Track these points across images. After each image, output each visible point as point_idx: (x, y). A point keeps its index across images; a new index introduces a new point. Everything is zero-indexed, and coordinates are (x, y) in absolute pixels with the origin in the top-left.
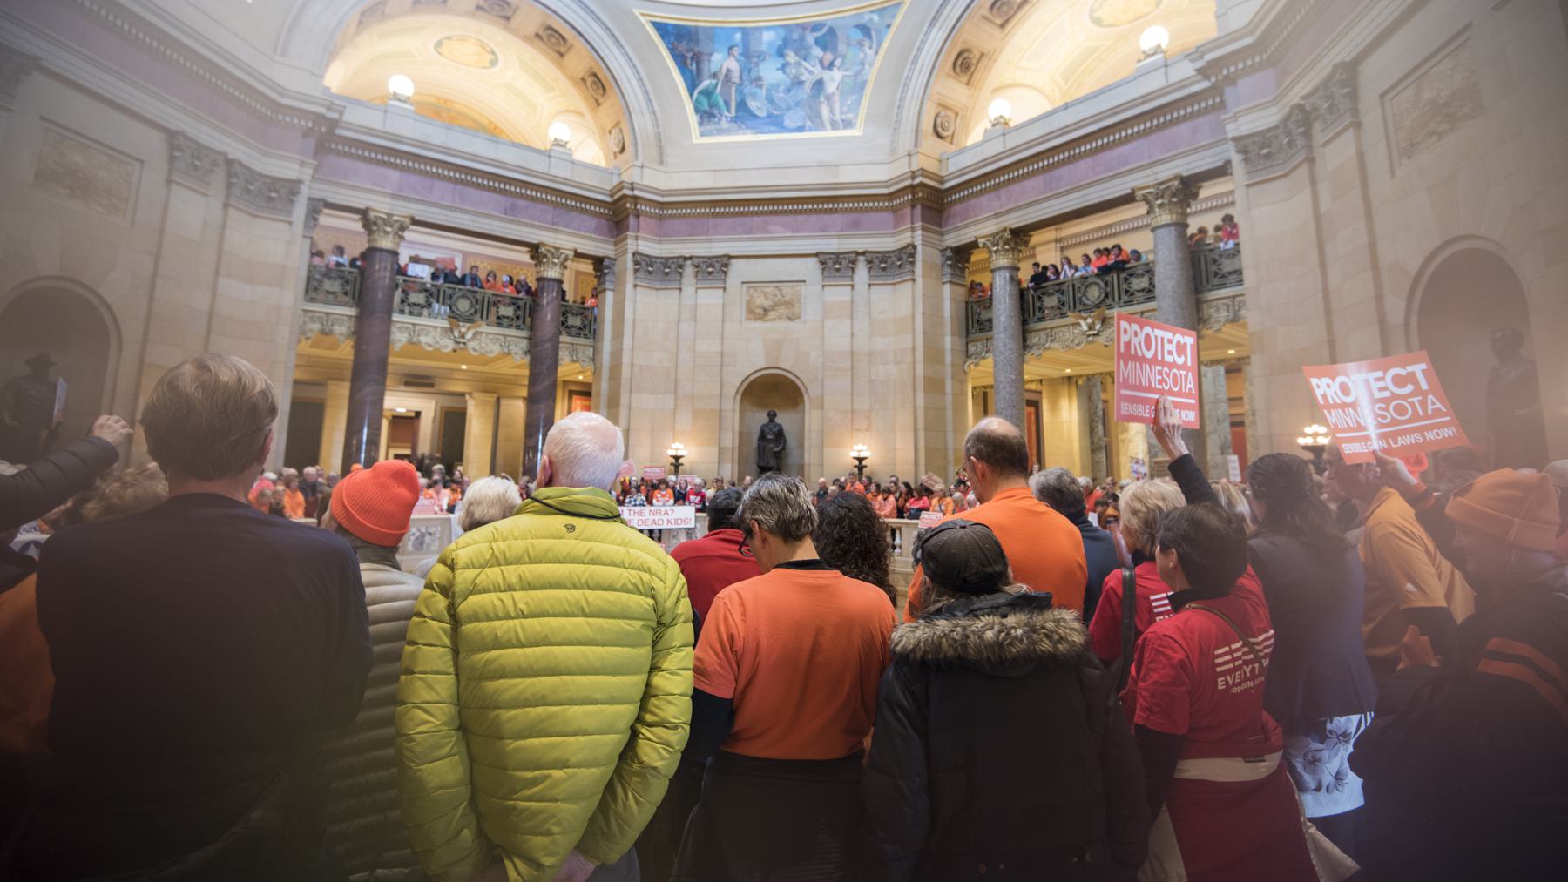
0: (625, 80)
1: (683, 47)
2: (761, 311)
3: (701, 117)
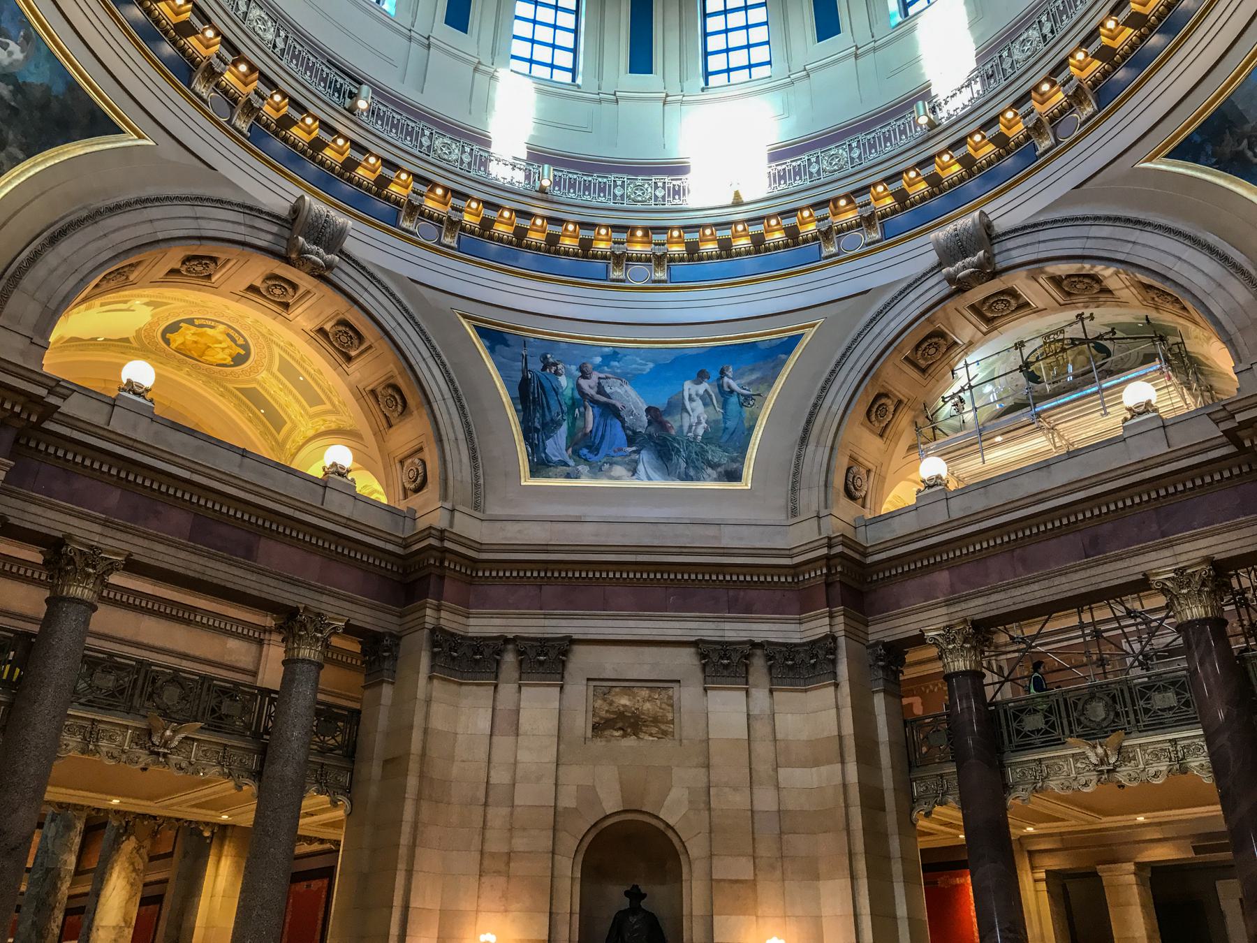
0: (1169, 262)
1: (1228, 147)
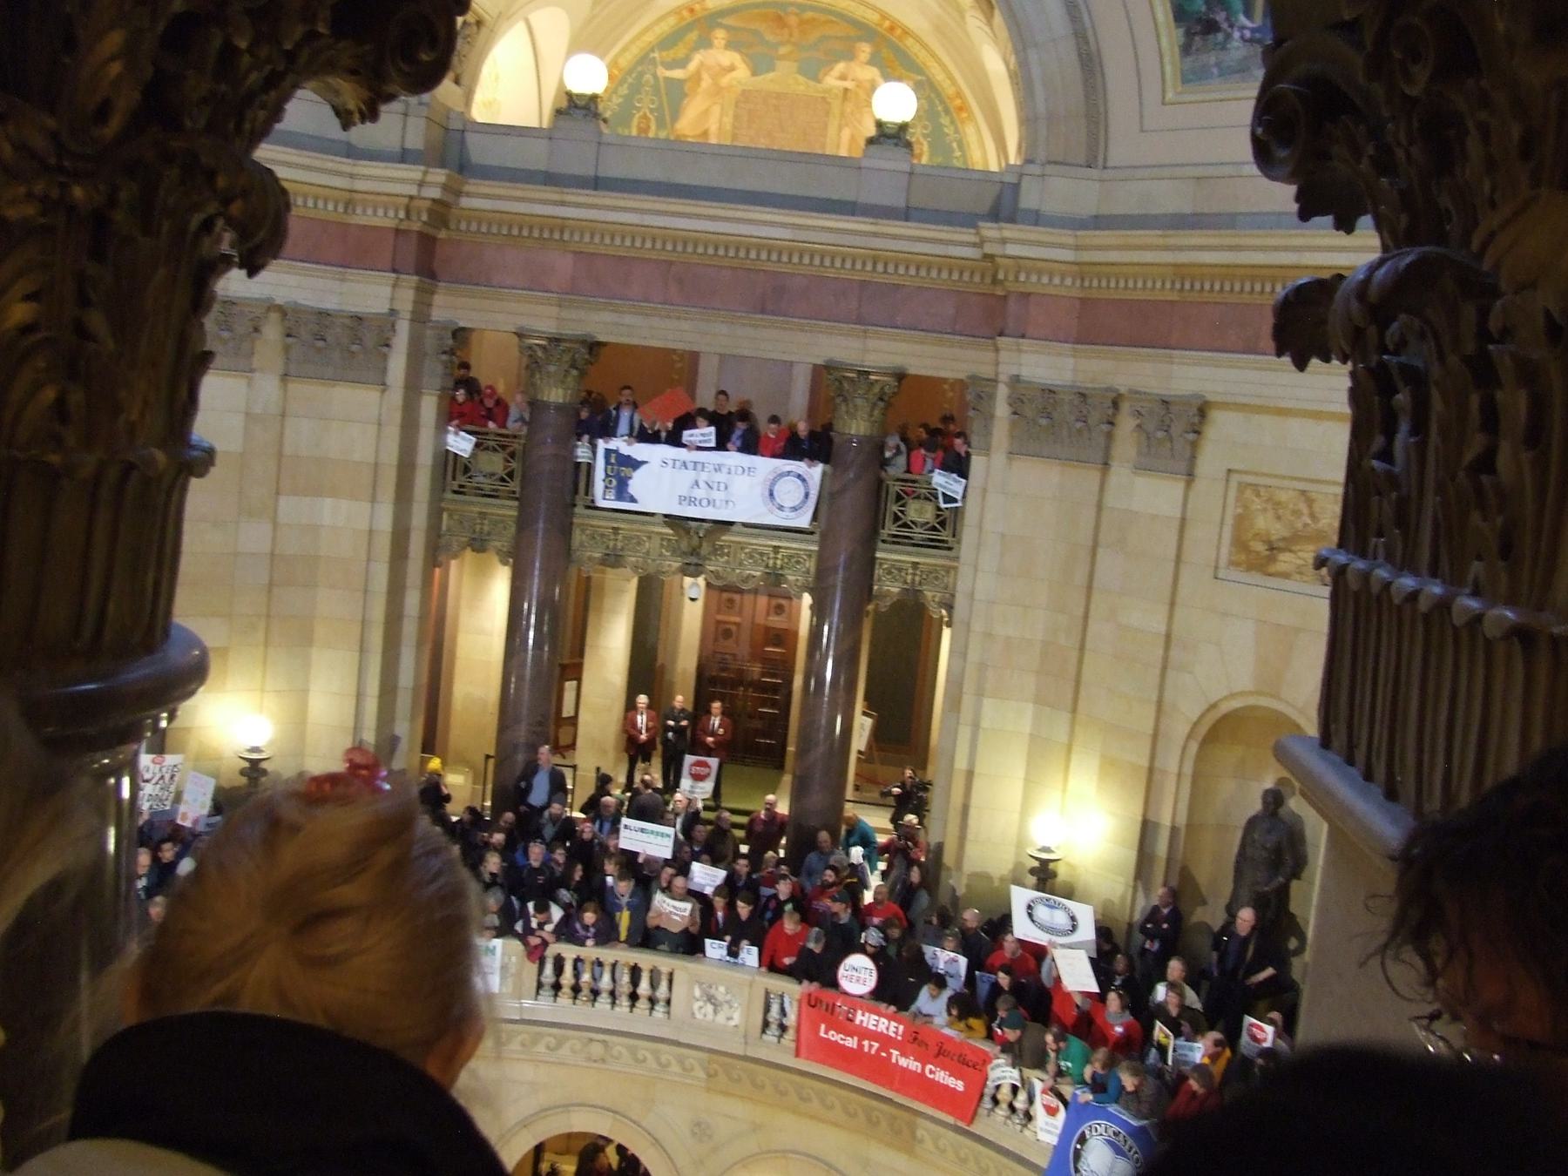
2: (1260, 547)
3: (1189, 35)
